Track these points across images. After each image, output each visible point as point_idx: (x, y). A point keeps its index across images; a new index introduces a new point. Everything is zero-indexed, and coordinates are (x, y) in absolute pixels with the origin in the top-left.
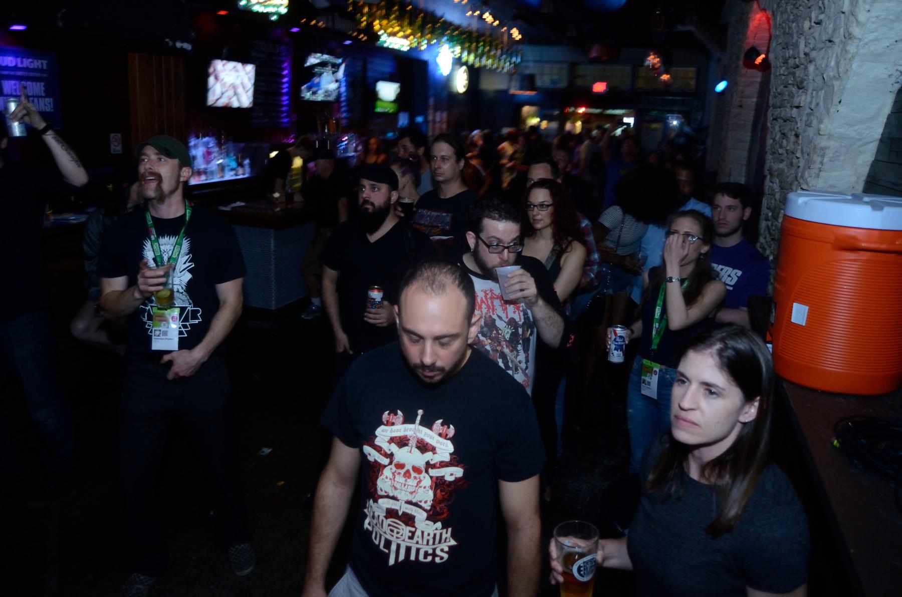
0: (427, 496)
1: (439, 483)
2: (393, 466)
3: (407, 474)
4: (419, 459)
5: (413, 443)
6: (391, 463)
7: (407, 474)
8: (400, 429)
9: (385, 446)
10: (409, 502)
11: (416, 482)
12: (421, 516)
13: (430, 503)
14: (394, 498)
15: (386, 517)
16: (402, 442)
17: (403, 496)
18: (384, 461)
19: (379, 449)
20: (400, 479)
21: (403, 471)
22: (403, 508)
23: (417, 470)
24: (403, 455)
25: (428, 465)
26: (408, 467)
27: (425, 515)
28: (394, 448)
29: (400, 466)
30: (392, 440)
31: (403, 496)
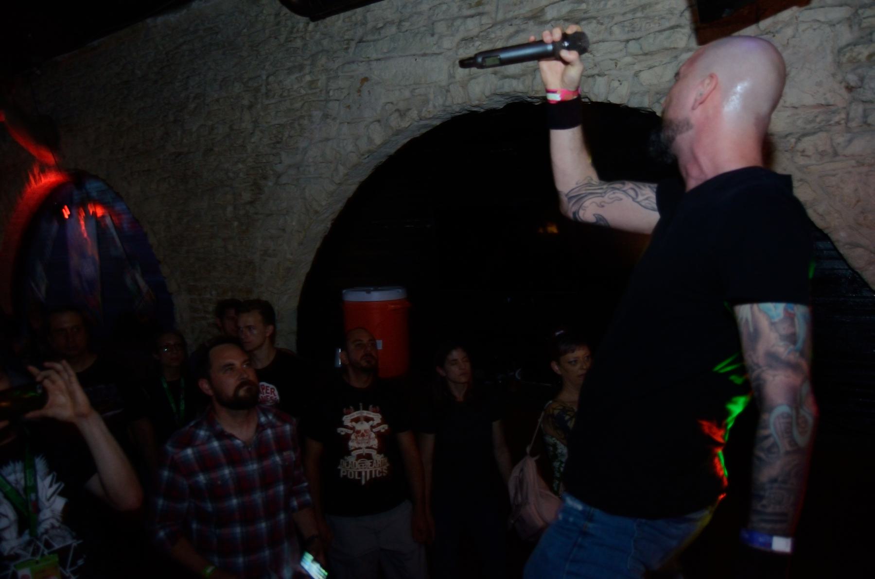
0: (375, 443)
1: (379, 435)
3: (363, 435)
5: (362, 419)
7: (363, 435)
8: (355, 414)
9: (349, 424)
10: (367, 448)
12: (374, 453)
14: (360, 448)
15: (357, 460)
16: (357, 420)
17: (363, 445)
18: (350, 432)
19: (346, 427)
24: (359, 427)
25: (372, 427)
28: (354, 424)
29: (358, 432)
30: (352, 421)
31: (363, 445)
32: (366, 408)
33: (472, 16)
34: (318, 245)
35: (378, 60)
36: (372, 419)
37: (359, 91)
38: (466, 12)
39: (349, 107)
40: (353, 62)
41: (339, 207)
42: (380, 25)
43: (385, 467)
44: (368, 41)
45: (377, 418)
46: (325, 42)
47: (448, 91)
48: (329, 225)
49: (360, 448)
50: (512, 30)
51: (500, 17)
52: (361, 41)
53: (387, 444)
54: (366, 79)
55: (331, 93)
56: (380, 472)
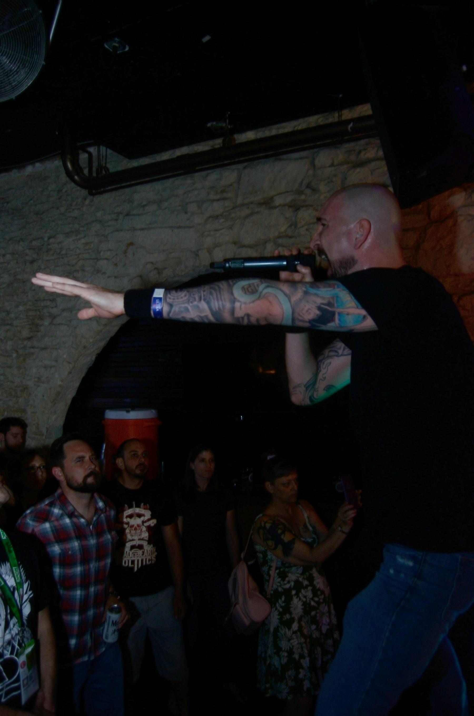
0: (145, 535)
1: (149, 528)
2: (129, 527)
3: (136, 529)
4: (139, 521)
6: (128, 526)
7: (136, 529)
10: (139, 539)
11: (140, 531)
13: (147, 537)
17: (136, 538)
20: (133, 532)
21: (133, 528)
22: (137, 543)
23: (138, 526)
26: (136, 526)
27: (147, 542)
29: (132, 526)
31: (136, 538)
32: (138, 506)
33: (218, 200)
34: (83, 375)
35: (142, 229)
36: (143, 515)
37: (125, 252)
38: (212, 197)
39: (116, 265)
40: (121, 230)
41: (103, 344)
42: (145, 203)
43: (154, 555)
44: (134, 215)
45: (148, 514)
46: (99, 214)
47: (197, 255)
48: (94, 358)
49: (133, 540)
50: (248, 212)
51: (239, 201)
52: (128, 215)
53: (155, 536)
54: (131, 244)
55: (102, 254)
56: (149, 560)
